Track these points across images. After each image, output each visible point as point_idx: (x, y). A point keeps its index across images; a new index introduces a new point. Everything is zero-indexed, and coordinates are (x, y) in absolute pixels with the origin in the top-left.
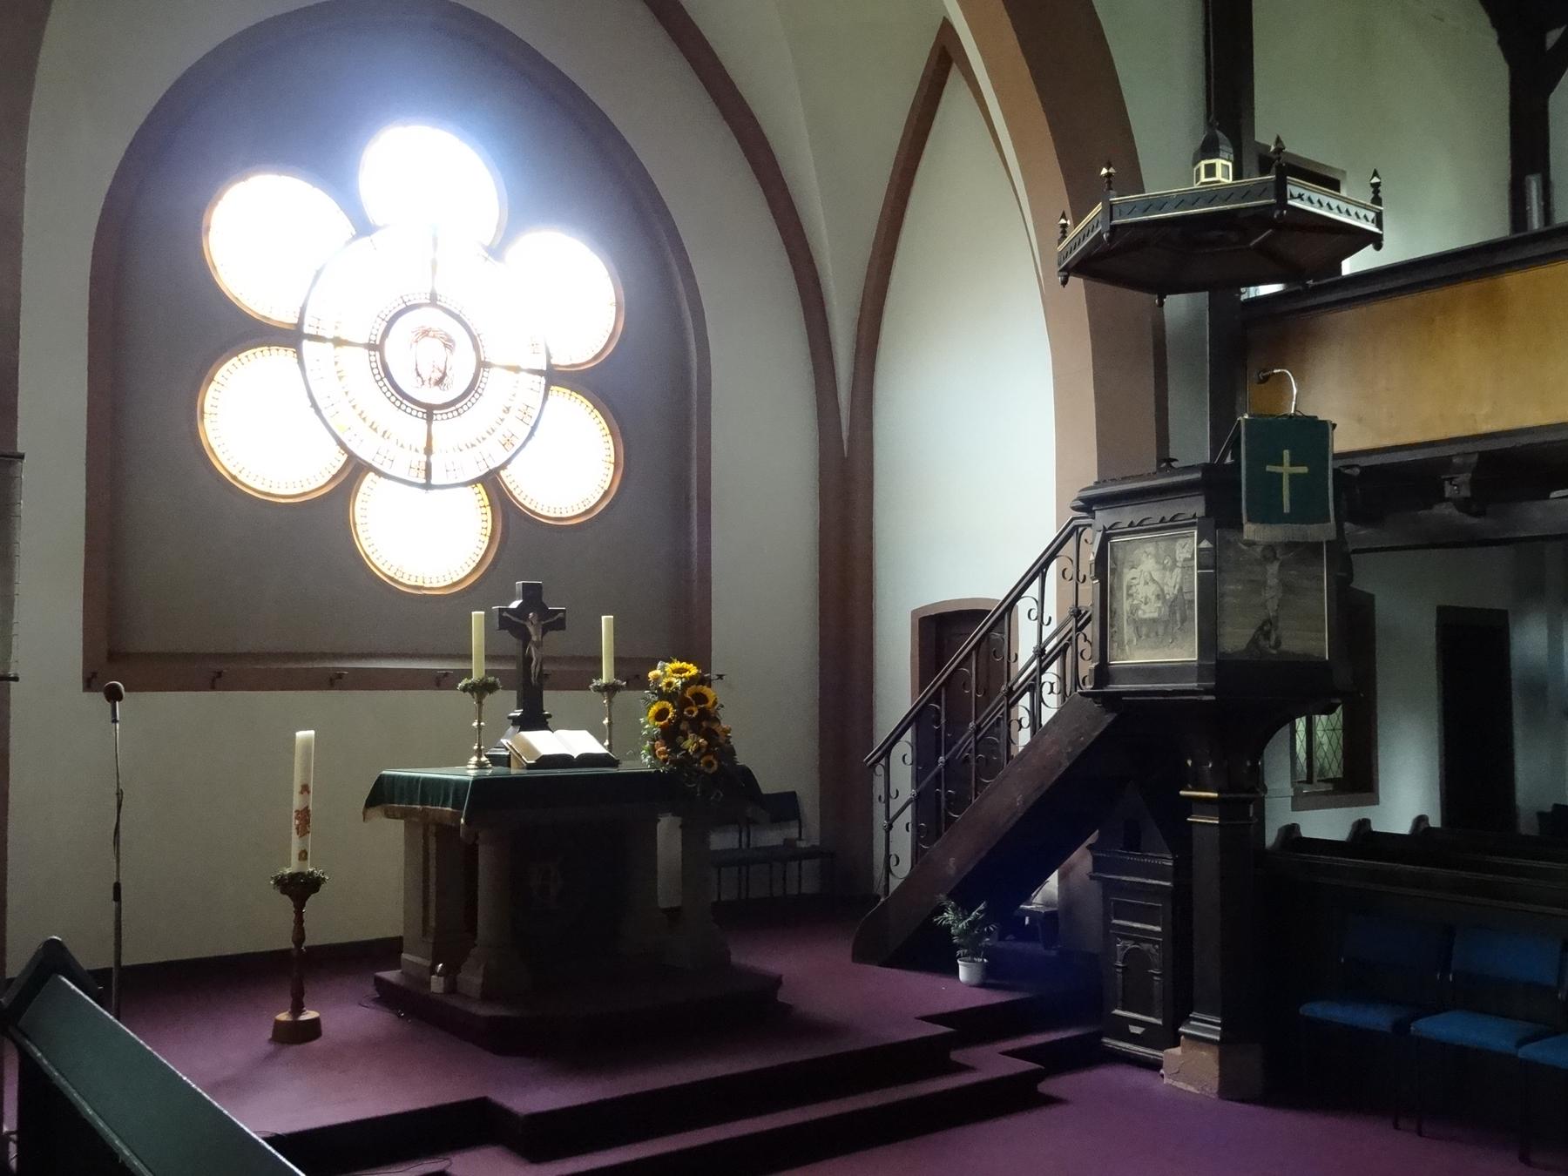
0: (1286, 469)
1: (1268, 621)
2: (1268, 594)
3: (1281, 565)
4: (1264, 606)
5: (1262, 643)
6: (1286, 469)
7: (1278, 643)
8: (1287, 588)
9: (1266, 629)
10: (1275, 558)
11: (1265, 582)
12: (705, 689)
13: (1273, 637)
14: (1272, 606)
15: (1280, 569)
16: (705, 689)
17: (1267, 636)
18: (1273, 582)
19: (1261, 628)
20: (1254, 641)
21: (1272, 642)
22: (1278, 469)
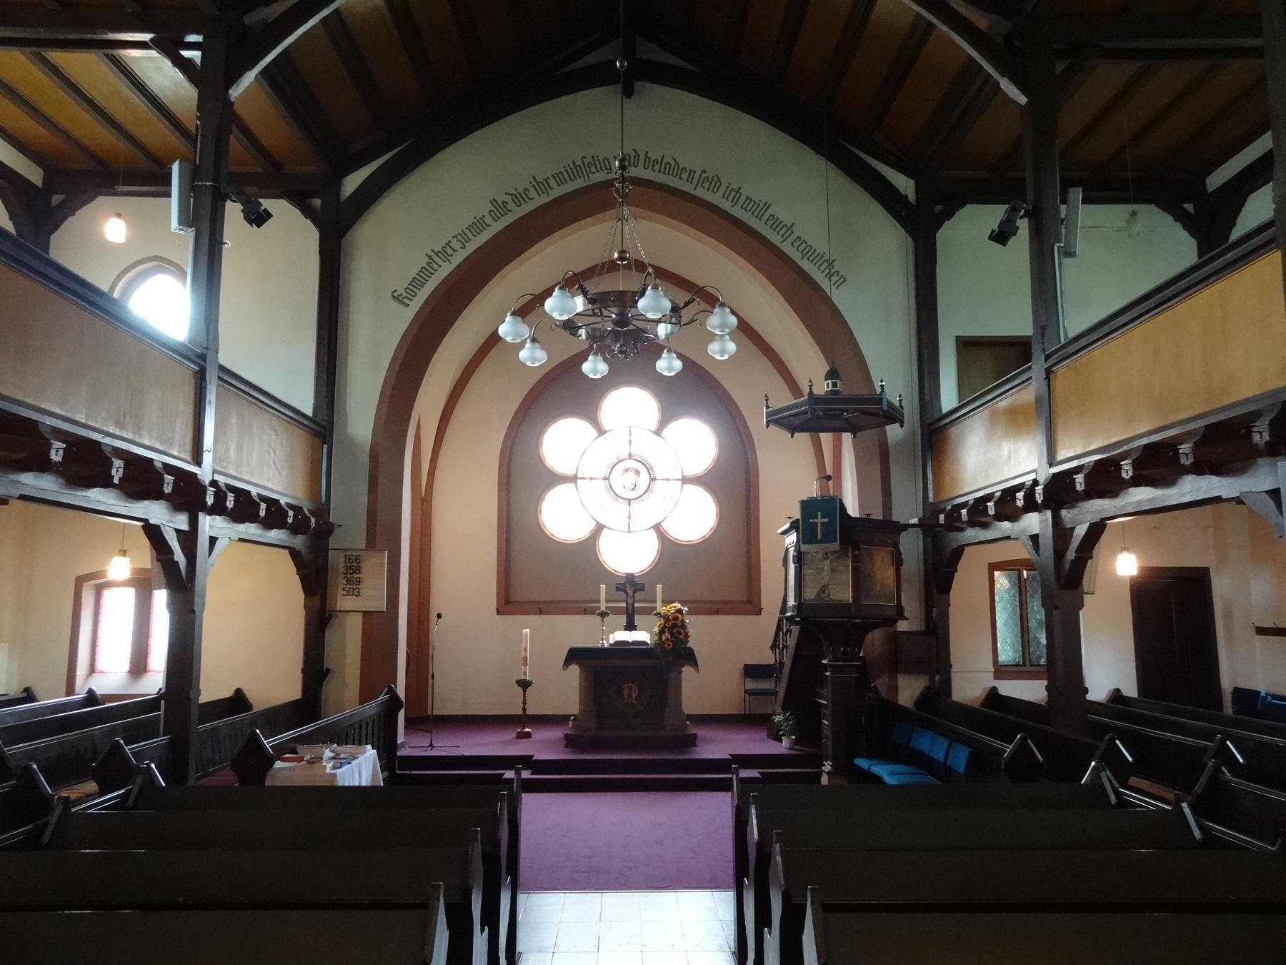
0: (819, 520)
1: (825, 586)
2: (825, 573)
3: (830, 561)
4: (823, 579)
5: (822, 595)
6: (819, 520)
7: (829, 595)
8: (833, 571)
9: (823, 589)
10: (828, 558)
11: (823, 569)
12: (680, 616)
13: (827, 592)
14: (826, 579)
15: (830, 564)
16: (680, 616)
17: (824, 592)
18: (827, 568)
19: (821, 589)
20: (818, 595)
21: (826, 595)
22: (815, 520)
